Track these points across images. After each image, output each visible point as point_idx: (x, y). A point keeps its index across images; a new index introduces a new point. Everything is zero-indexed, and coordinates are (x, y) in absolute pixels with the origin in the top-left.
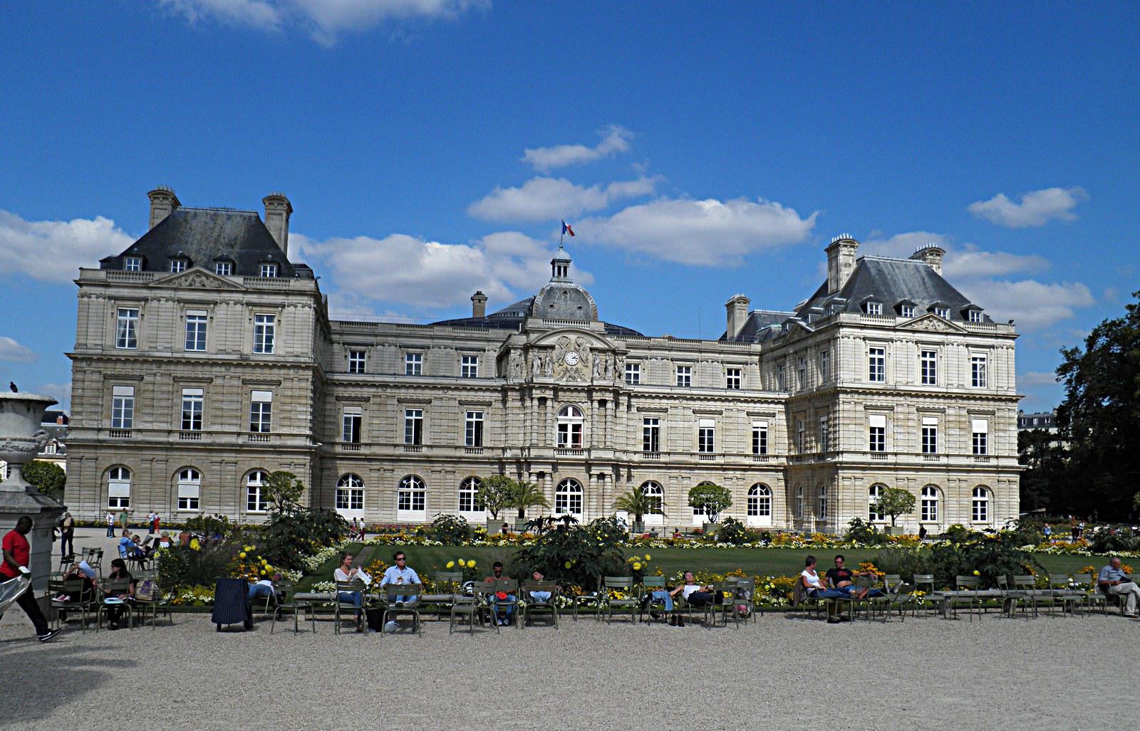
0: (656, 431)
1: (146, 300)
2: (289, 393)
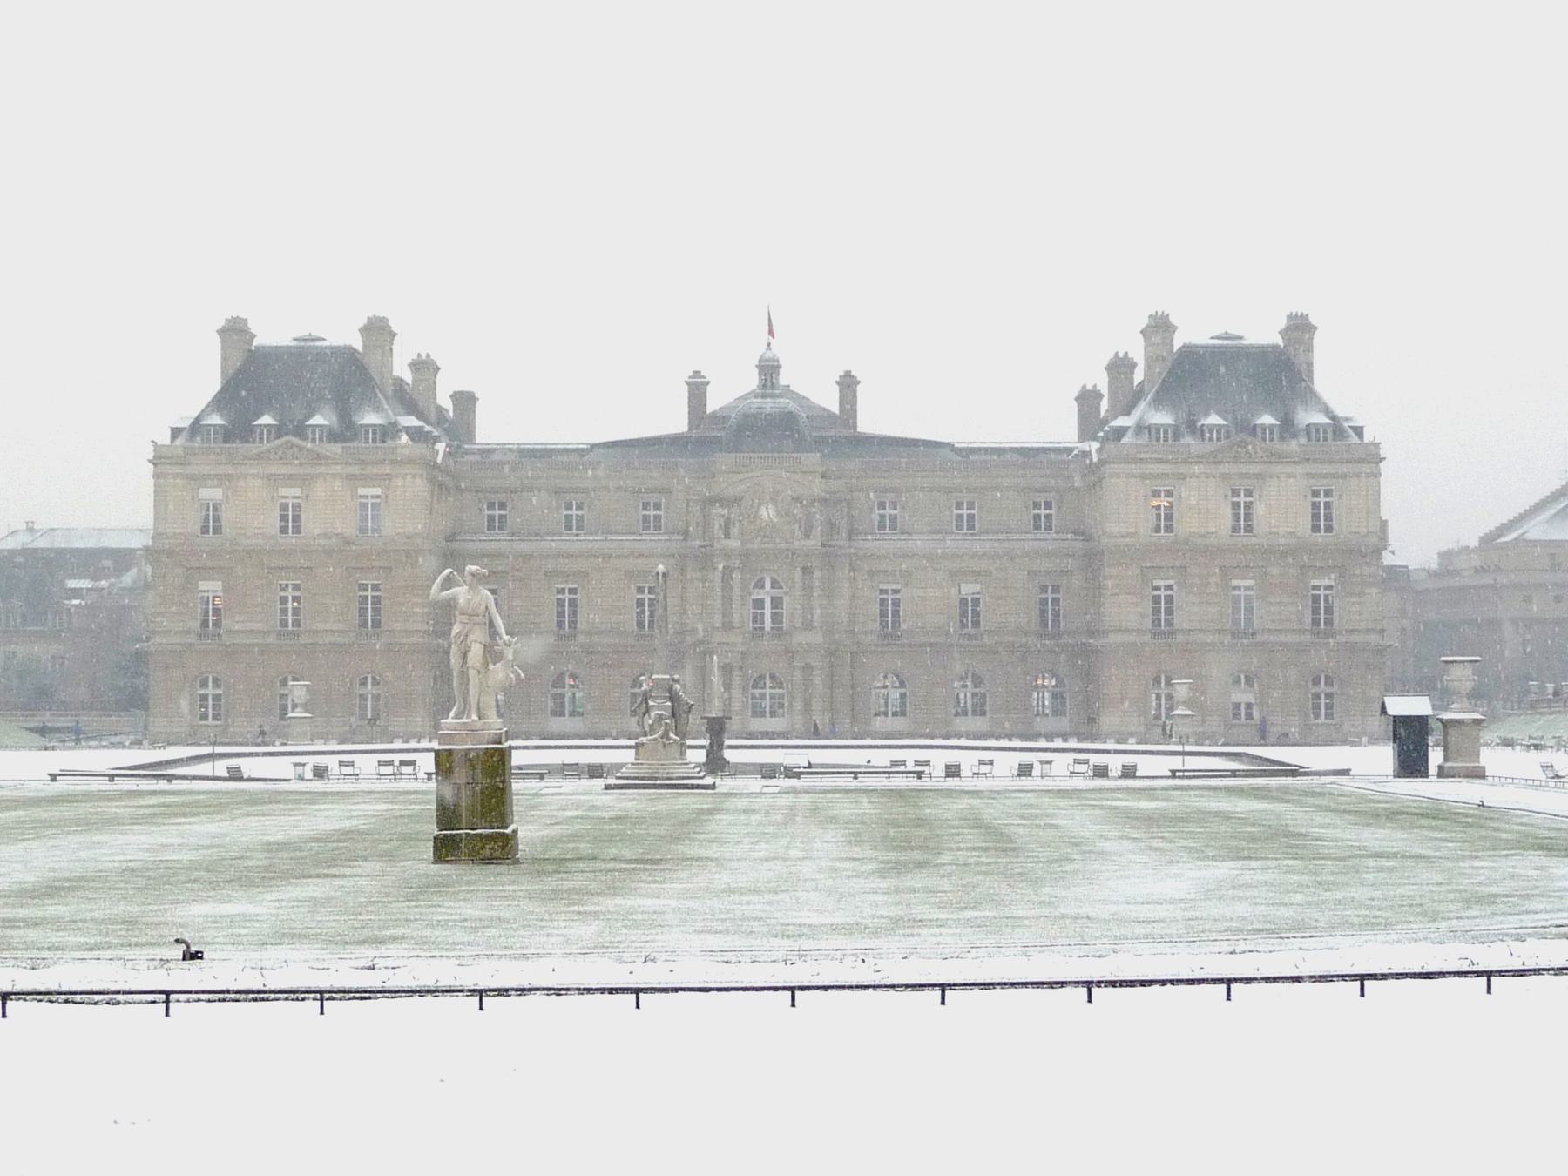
0: (896, 603)
1: (229, 477)
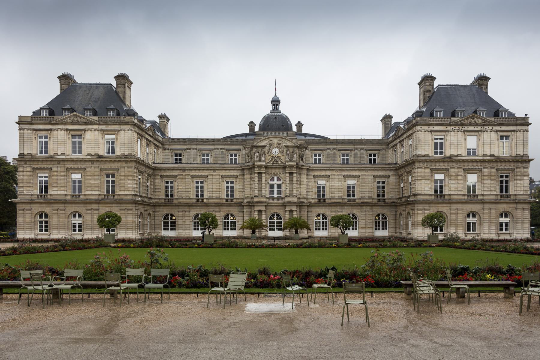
2: (123, 174)
